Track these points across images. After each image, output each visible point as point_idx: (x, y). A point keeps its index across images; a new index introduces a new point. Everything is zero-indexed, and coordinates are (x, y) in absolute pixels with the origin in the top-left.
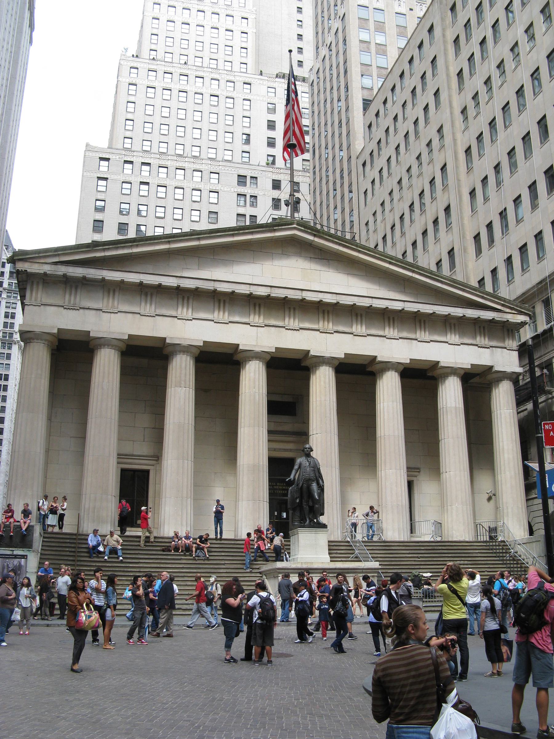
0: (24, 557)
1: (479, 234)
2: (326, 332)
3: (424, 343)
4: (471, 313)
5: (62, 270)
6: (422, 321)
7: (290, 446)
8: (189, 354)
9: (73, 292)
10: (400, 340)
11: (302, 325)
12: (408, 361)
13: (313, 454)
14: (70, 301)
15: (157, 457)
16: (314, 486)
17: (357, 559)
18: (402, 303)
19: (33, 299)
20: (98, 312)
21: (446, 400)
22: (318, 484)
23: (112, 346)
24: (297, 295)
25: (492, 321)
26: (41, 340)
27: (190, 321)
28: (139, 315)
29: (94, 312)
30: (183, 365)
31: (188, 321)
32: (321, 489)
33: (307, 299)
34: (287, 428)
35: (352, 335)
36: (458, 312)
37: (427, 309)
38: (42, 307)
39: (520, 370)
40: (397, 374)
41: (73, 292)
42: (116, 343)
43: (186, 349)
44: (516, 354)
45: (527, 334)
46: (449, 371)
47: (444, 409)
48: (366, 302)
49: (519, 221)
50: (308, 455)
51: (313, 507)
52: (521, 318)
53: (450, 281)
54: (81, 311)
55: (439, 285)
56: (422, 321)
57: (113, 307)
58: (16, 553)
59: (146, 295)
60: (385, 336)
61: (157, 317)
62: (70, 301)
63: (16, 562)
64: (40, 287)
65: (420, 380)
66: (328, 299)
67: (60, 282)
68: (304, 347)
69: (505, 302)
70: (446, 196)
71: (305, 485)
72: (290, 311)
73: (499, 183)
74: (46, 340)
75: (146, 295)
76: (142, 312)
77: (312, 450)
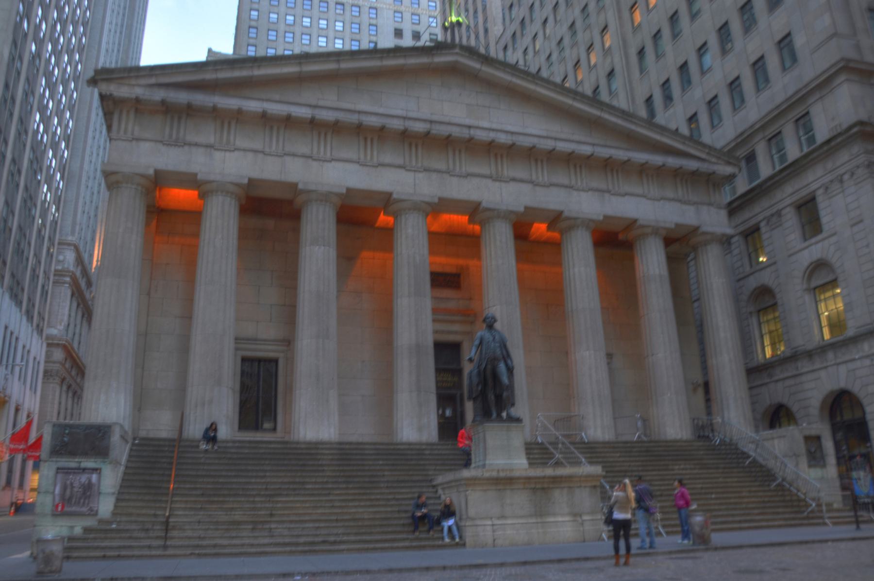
1: (651, 97)
4: (672, 162)
5: (159, 95)
7: (456, 327)
9: (175, 125)
10: (590, 193)
12: (601, 218)
13: (498, 326)
14: (171, 136)
15: (289, 342)
16: (502, 367)
17: (558, 464)
19: (122, 132)
22: (507, 365)
24: (465, 133)
25: (695, 174)
28: (260, 156)
29: (201, 150)
32: (510, 370)
33: (476, 137)
34: (452, 305)
35: (530, 186)
36: (657, 159)
37: (621, 154)
38: (134, 142)
39: (729, 231)
41: (175, 125)
43: (325, 197)
44: (723, 213)
45: (742, 186)
48: (548, 144)
49: (703, 73)
50: (490, 327)
51: (501, 396)
52: (729, 170)
54: (186, 148)
55: (633, 127)
57: (228, 142)
58: (83, 465)
59: (271, 128)
62: (171, 136)
63: (84, 478)
64: (132, 115)
65: (614, 243)
66: (503, 138)
68: (474, 196)
69: (710, 149)
70: (609, 60)
71: (489, 367)
72: (454, 155)
73: (675, 35)
75: (271, 128)
76: (267, 150)
77: (495, 321)
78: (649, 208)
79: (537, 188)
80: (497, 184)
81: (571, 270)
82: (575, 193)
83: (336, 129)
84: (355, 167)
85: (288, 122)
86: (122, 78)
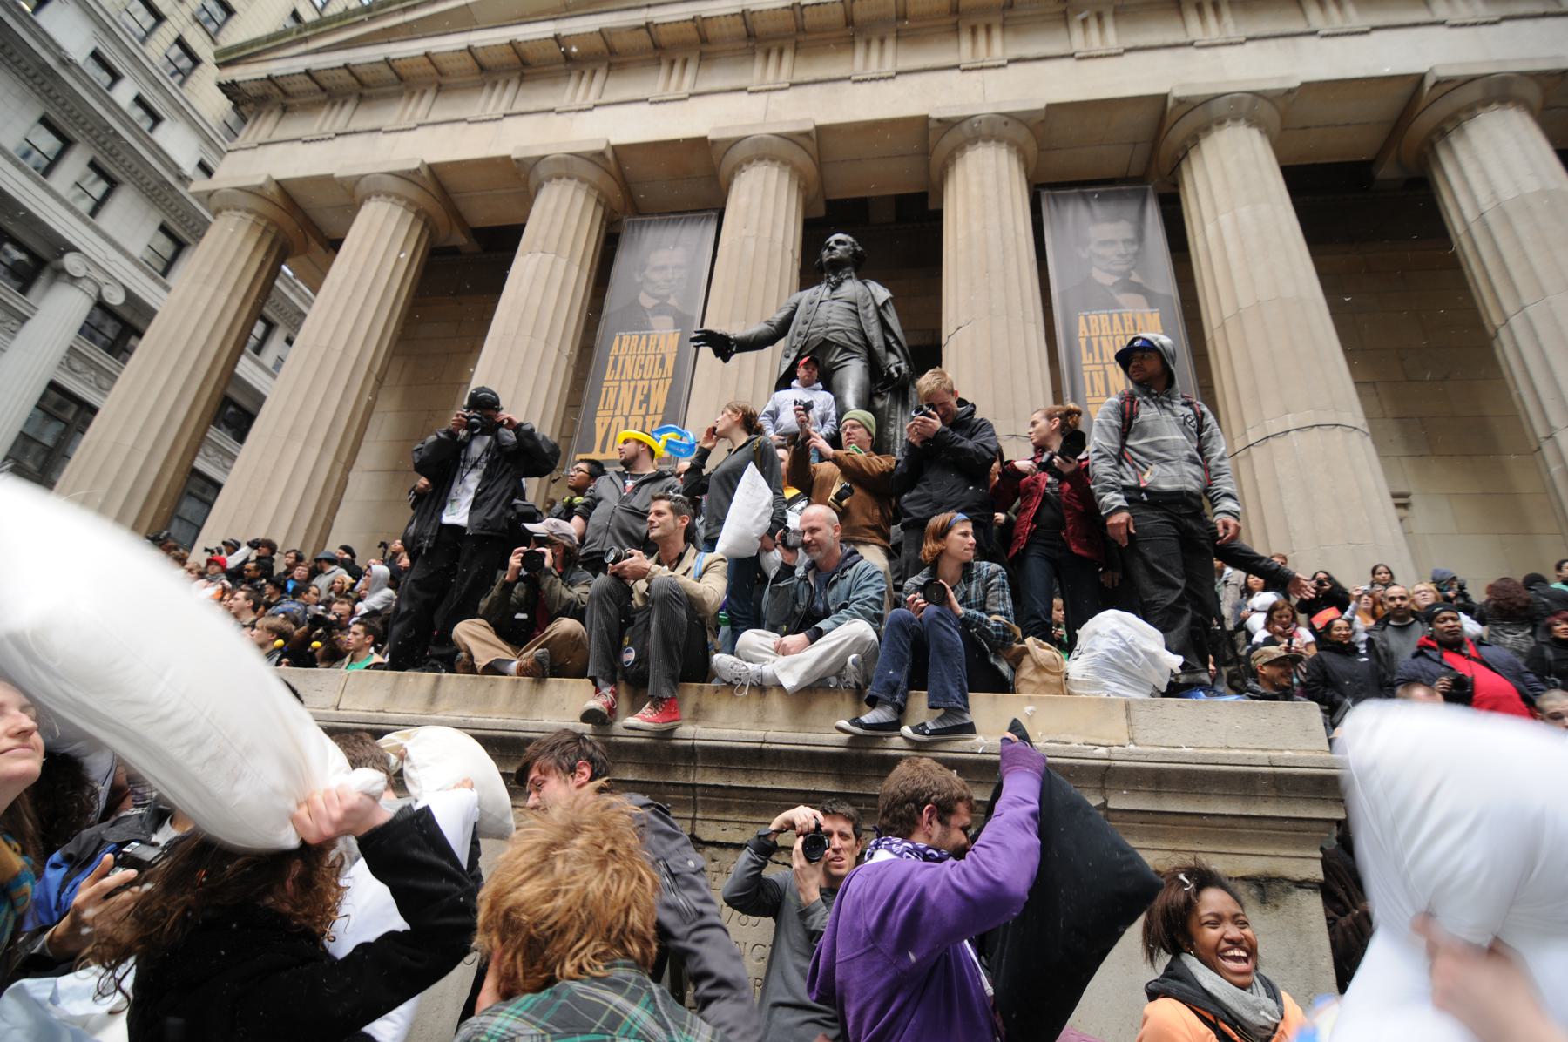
2: (982, 68)
8: (575, 182)
10: (1250, 45)
11: (903, 64)
20: (374, 135)
21: (1488, 182)
23: (388, 195)
26: (238, 210)
27: (588, 114)
30: (551, 205)
31: (582, 115)
40: (1255, 133)
46: (1474, 93)
47: (1490, 217)
59: (495, 84)
60: (1191, 44)
61: (507, 120)
67: (321, 104)
74: (249, 211)
80: (975, 74)
81: (1210, 227)
82: (1205, 53)
84: (645, 106)
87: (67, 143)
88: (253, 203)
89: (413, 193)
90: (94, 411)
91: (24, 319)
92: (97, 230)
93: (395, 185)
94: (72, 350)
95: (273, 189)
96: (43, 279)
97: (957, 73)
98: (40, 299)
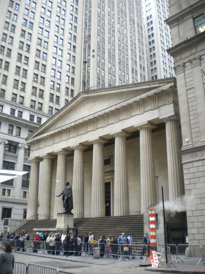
0: (7, 228)
3: (128, 119)
4: (143, 96)
6: (128, 109)
18: (115, 106)
22: (68, 196)
35: (102, 128)
36: (138, 98)
37: (125, 104)
40: (119, 138)
42: (45, 157)
53: (133, 85)
55: (130, 89)
56: (128, 109)
61: (54, 145)
78: (138, 119)
79: (104, 128)
83: (60, 133)
85: (53, 136)
86: (28, 139)
87: (13, 126)
88: (34, 160)
89: (47, 157)
90: (30, 166)
91: (17, 157)
92: (21, 138)
93: (45, 157)
94: (24, 159)
95: (35, 158)
96: (17, 149)
97: (92, 132)
98: (18, 153)
